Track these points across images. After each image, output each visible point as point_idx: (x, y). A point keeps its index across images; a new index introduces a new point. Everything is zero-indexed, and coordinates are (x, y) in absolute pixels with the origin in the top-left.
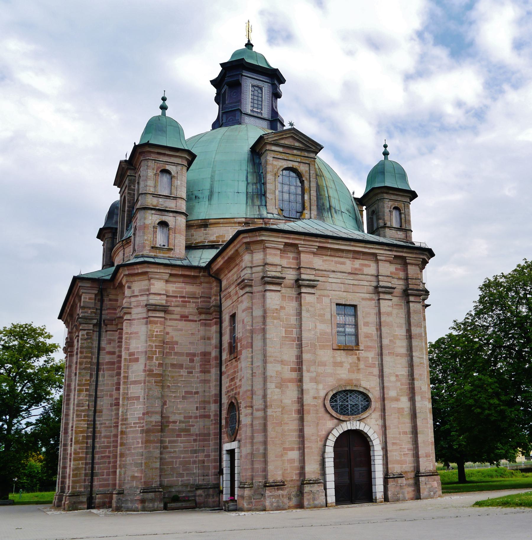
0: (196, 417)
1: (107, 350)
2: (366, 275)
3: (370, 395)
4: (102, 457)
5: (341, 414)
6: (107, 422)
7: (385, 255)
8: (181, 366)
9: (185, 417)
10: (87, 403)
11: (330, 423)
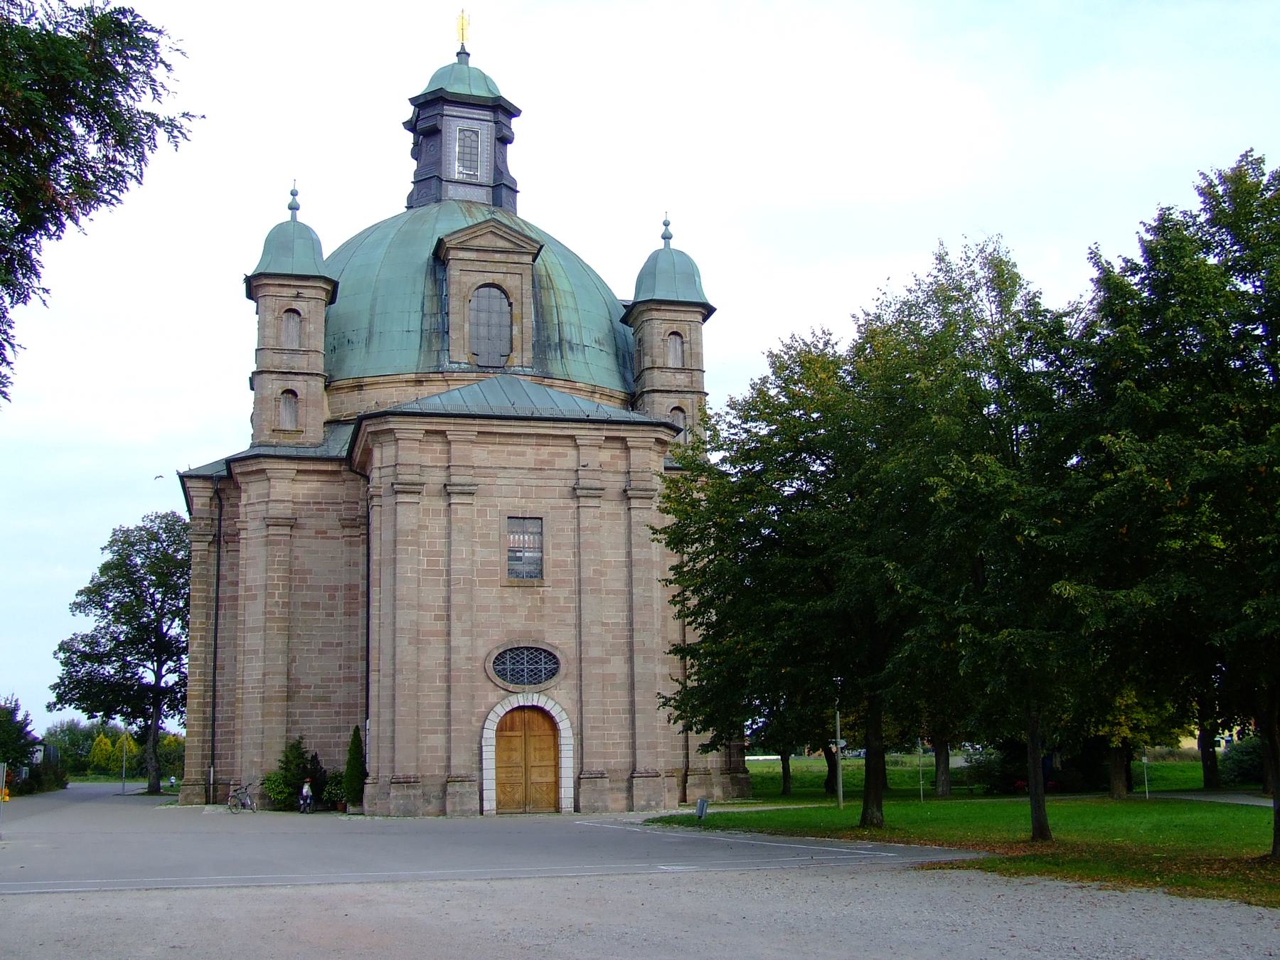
0: (339, 680)
1: (229, 580)
2: (558, 470)
3: (558, 655)
4: (225, 732)
5: (512, 681)
6: (231, 683)
8: (316, 606)
10: (203, 655)
11: (492, 696)
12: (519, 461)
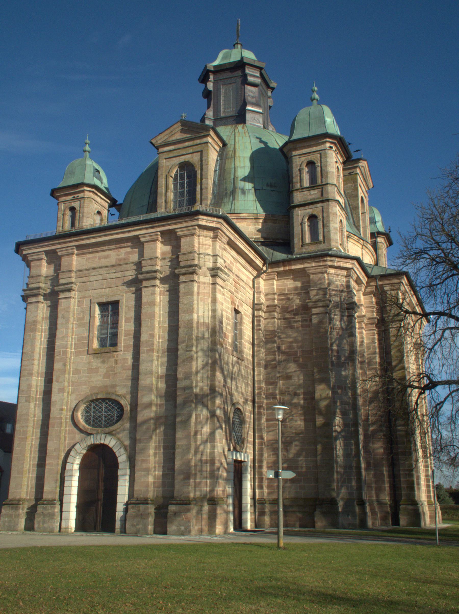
7: (148, 235)
12: (105, 262)
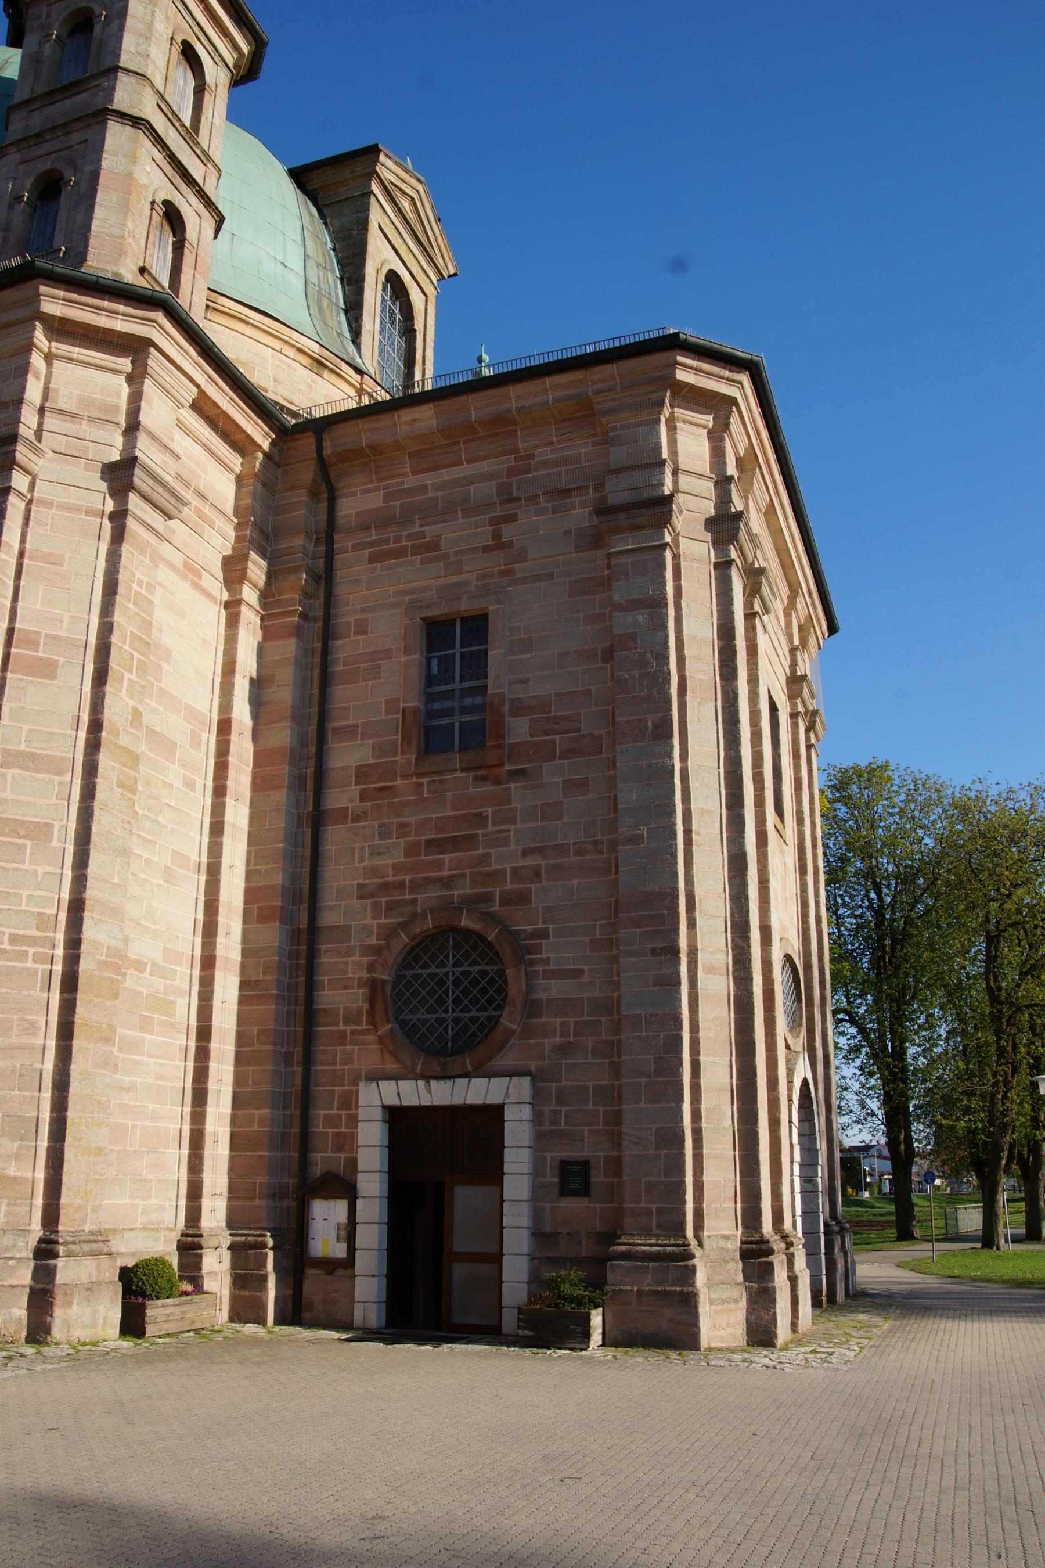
9: (165, 951)
